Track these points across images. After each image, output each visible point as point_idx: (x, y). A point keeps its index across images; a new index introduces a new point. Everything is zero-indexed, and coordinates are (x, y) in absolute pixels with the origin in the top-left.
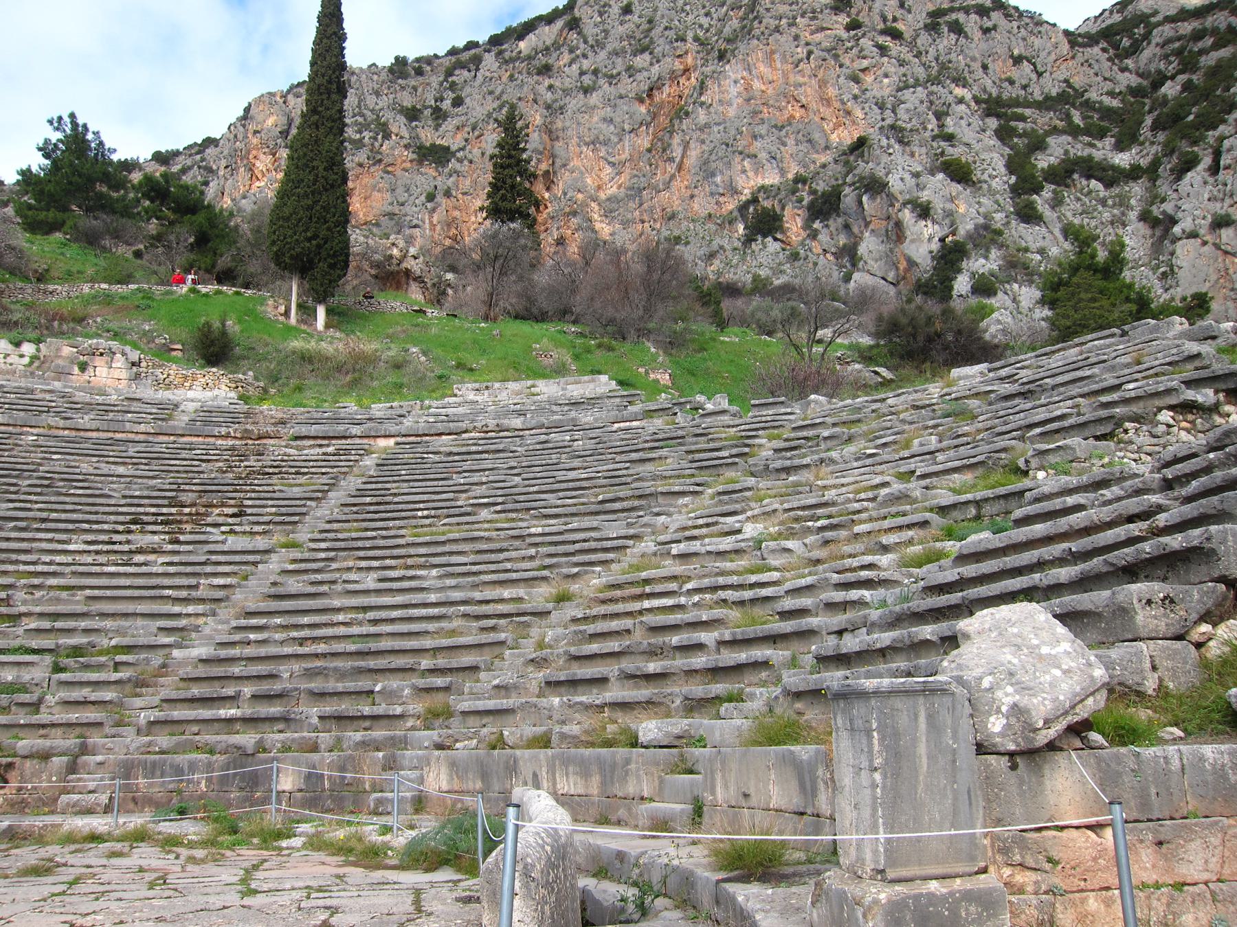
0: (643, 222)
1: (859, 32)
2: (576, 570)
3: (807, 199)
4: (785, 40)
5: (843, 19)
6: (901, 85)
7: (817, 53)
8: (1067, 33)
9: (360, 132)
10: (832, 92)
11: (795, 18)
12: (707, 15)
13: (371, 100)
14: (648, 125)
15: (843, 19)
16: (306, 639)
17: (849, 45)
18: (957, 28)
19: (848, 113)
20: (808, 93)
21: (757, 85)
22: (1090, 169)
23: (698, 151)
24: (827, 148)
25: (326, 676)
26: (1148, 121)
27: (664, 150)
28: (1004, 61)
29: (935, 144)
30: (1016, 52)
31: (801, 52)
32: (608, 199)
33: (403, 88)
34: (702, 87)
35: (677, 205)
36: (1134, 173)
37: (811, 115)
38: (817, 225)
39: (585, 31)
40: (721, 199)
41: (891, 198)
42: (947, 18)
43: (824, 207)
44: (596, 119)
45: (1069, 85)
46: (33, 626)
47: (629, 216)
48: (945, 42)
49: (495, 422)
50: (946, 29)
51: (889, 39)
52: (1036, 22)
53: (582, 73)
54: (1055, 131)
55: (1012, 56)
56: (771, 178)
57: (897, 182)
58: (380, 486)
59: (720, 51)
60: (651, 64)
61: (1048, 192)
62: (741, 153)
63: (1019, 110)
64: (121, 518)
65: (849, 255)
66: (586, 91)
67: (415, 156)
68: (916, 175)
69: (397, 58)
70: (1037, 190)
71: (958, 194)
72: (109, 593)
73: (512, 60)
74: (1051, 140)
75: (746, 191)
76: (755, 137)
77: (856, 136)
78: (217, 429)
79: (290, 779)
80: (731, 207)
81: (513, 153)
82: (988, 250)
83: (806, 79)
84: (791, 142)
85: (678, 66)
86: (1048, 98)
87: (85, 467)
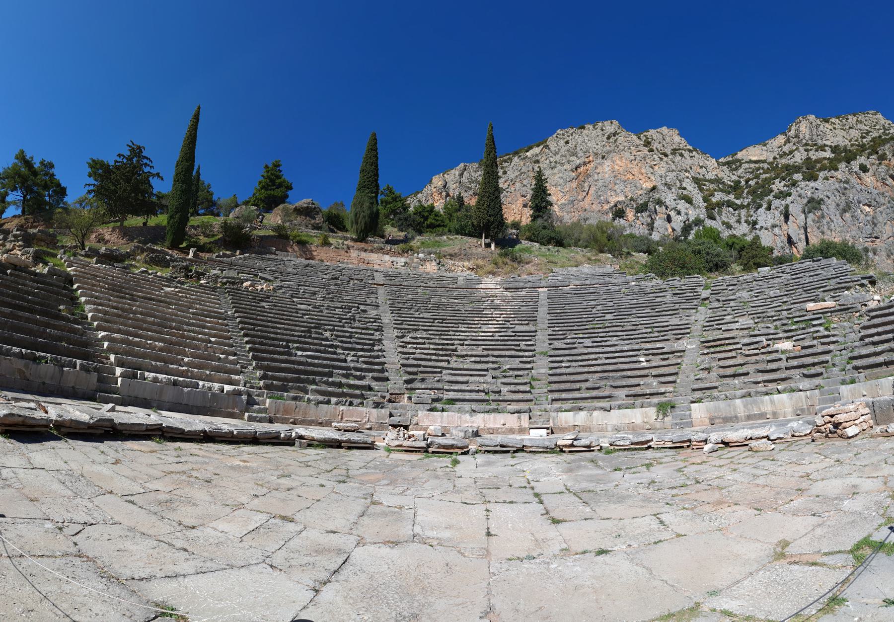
4: (627, 154)
10: (643, 171)
20: (635, 171)
21: (616, 167)
22: (729, 204)
26: (746, 191)
34: (596, 168)
36: (742, 207)
43: (641, 208)
56: (621, 198)
65: (651, 226)
68: (675, 200)
70: (714, 209)
76: (615, 184)
84: (628, 186)
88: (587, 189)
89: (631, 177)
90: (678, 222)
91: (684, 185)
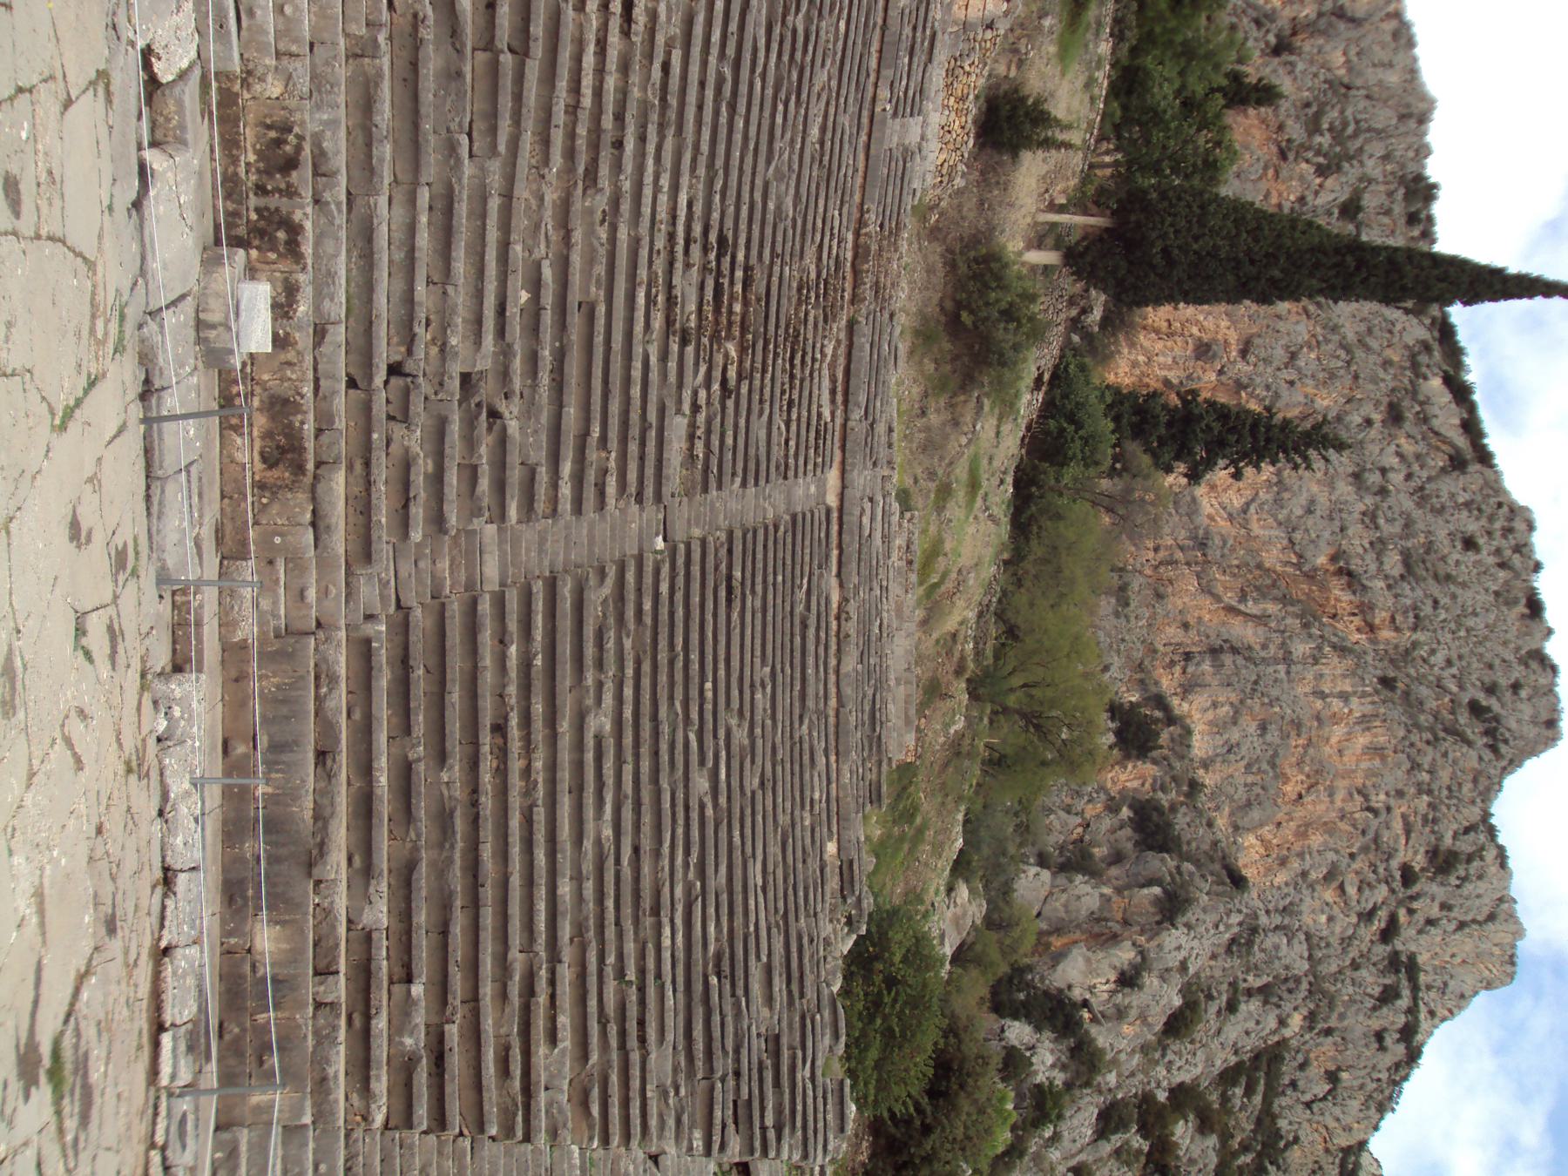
0: (1156, 550)
1: (1397, 884)
2: (595, 1110)
3: (1164, 799)
4: (1396, 776)
5: (1419, 862)
6: (1315, 941)
7: (1374, 823)
8: (1362, 1144)
9: (1330, 130)
10: (1316, 840)
11: (1429, 792)
12: (1449, 663)
13: (1378, 149)
14: (1298, 566)
15: (1419, 862)
16: (505, 737)
17: (1381, 870)
18: (1388, 996)
19: (1283, 862)
20: (1318, 806)
21: (1338, 732)
24: (1236, 828)
25: (441, 846)
27: (1257, 588)
28: (1334, 1059)
29: (1225, 987)
30: (1344, 1075)
31: (1379, 800)
32: (1194, 500)
33: (1390, 194)
34: (1342, 650)
35: (1175, 602)
37: (1286, 809)
38: (1126, 812)
39: (1447, 479)
41: (1155, 930)
42: (1405, 983)
43: (1151, 827)
44: (1315, 488)
45: (1286, 1146)
46: (547, 273)
47: (1167, 530)
48: (1370, 979)
49: (852, 632)
50: (1388, 981)
51: (1383, 925)
52: (1384, 1104)
53: (1383, 471)
54: (1225, 1137)
55: (1339, 1069)
56: (1200, 745)
57: (1175, 942)
58: (760, 565)
59: (1394, 680)
60: (1386, 577)
61: (1139, 1143)
62: (1242, 702)
63: (1261, 1088)
64: (729, 223)
65: (1074, 861)
66: (1357, 477)
67: (1286, 210)
68: (1183, 967)
69: (1434, 186)
70: (1144, 1131)
71: (1149, 1025)
72: (599, 339)
73: (1415, 366)
74: (1212, 1141)
75: (1185, 706)
76: (1263, 728)
77: (1248, 873)
78: (873, 207)
81: (1274, 446)
82: (1064, 1068)
83: (1339, 804)
85: (1380, 616)
86: (1274, 1117)
87: (821, 77)
88: (1251, 607)
89: (1290, 789)
90: (1082, 974)
91: (1250, 1007)
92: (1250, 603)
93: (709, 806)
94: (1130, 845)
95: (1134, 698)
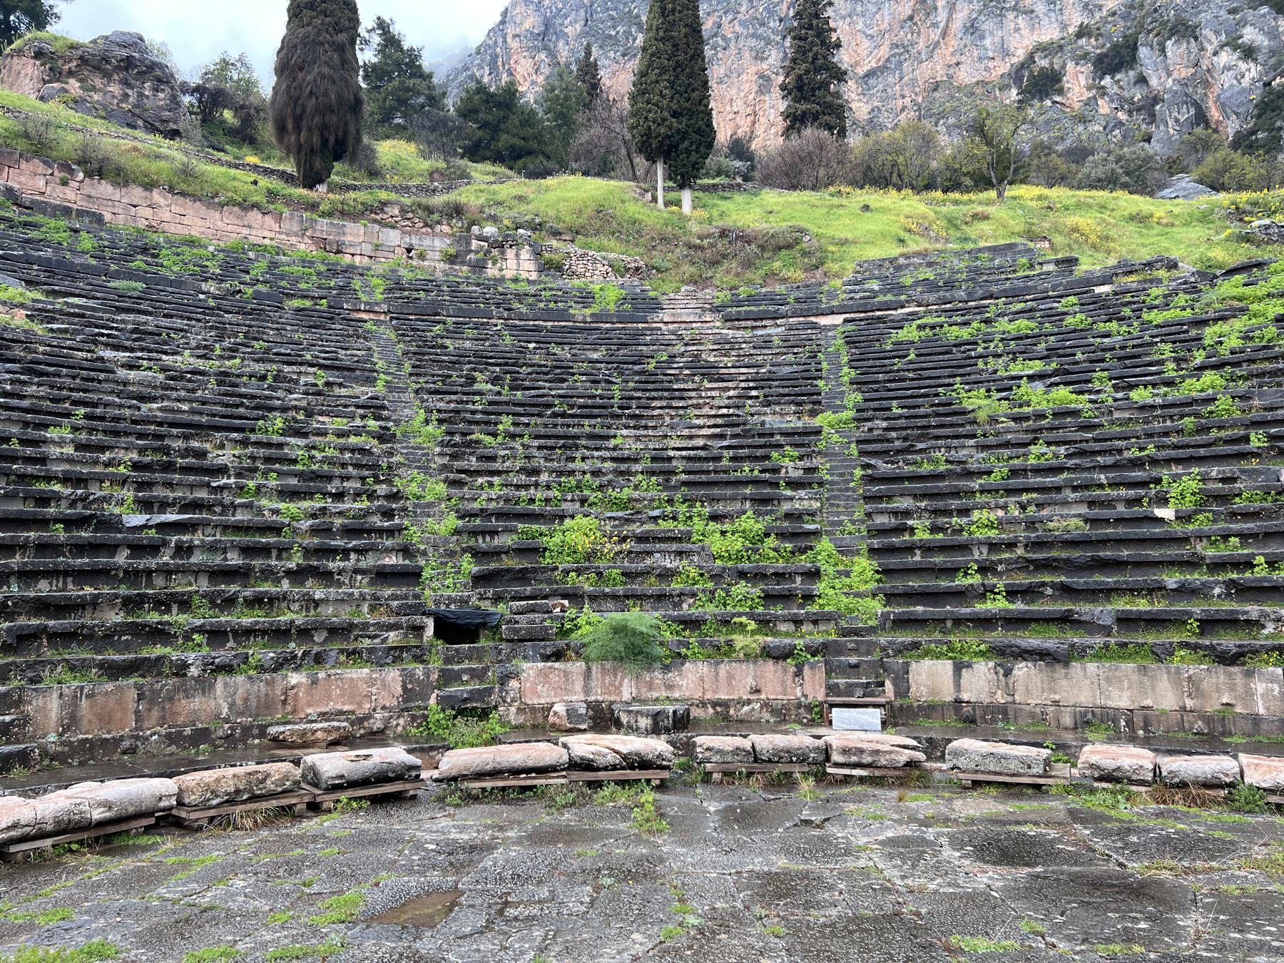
0: (903, 97)
9: (614, 27)
23: (966, 12)
38: (1107, 81)
40: (991, 64)
56: (1049, 33)
79: (1127, 694)
80: (1001, 71)
92: (939, 19)
93: (1052, 380)
94: (1131, 73)
95: (1014, 91)
